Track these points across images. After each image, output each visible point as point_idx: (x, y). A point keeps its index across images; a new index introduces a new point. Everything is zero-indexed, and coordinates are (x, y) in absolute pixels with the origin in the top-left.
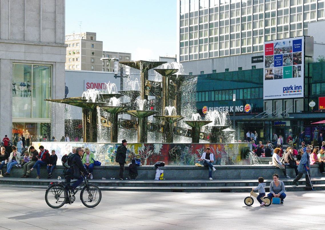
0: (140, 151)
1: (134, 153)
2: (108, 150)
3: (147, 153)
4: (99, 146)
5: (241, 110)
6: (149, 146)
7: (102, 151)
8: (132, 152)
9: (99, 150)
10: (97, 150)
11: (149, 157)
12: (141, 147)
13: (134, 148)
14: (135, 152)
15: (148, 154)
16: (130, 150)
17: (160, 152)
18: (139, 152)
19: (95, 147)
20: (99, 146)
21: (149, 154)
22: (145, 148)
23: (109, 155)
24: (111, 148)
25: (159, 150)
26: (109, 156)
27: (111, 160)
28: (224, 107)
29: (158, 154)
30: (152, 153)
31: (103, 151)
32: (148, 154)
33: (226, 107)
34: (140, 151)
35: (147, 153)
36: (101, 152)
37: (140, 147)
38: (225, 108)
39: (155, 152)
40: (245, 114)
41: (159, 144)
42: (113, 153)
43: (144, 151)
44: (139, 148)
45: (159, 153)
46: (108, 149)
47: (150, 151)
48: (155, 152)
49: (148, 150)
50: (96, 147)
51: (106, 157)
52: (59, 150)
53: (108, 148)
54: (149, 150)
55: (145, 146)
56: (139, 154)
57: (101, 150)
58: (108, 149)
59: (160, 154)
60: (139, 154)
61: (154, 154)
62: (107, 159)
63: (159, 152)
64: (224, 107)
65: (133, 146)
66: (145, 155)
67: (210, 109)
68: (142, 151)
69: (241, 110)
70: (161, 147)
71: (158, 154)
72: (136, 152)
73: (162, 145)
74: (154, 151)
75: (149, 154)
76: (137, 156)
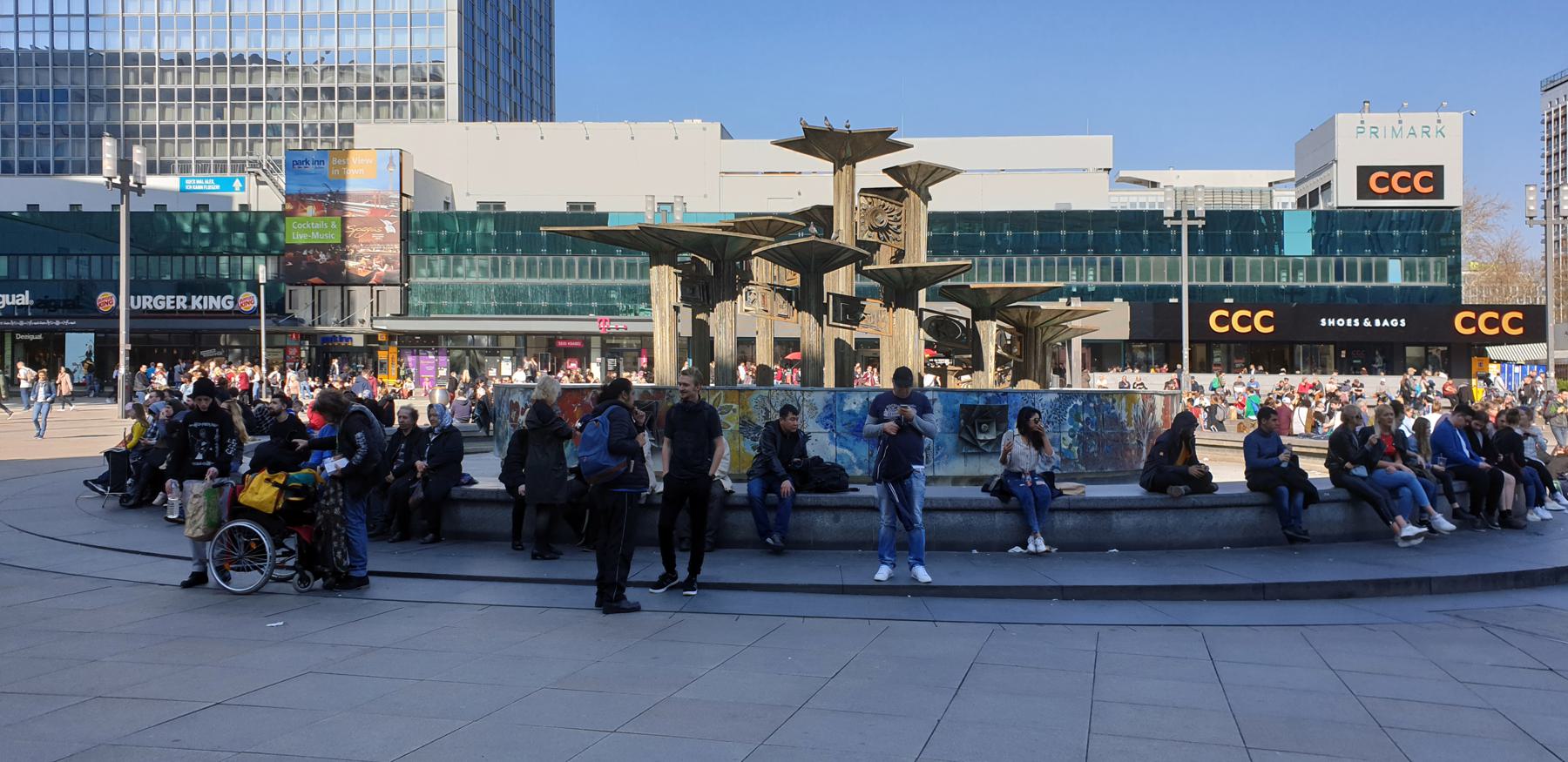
5: (228, 305)
7: (1051, 419)
13: (1125, 406)
24: (1075, 406)
28: (173, 297)
33: (179, 298)
36: (1048, 423)
38: (175, 299)
40: (237, 315)
42: (1080, 424)
46: (1068, 410)
51: (1064, 439)
57: (1050, 417)
58: (1068, 410)
64: (173, 297)
67: (148, 300)
69: (228, 305)
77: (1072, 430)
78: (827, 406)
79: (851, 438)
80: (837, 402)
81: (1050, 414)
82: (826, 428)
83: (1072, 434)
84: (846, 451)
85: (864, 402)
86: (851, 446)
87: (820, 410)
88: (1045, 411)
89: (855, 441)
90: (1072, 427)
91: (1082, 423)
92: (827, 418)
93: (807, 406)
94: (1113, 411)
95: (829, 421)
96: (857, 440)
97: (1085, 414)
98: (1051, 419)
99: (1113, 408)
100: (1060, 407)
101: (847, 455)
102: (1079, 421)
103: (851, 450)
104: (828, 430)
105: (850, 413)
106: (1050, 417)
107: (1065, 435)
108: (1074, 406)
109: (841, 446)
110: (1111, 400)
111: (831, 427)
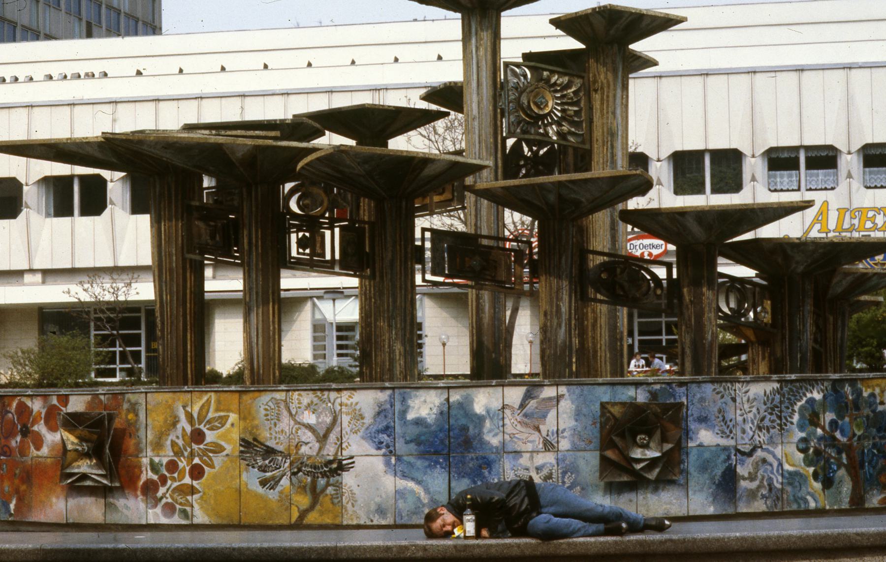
2: (796, 418)
4: (751, 394)
7: (767, 423)
9: (751, 415)
10: (740, 419)
19: (727, 399)
20: (751, 394)
23: (801, 446)
24: (811, 401)
26: (801, 451)
27: (811, 470)
31: (773, 421)
36: (760, 428)
42: (819, 431)
46: (796, 408)
50: (734, 400)
52: (465, 429)
53: (799, 404)
57: (762, 419)
62: (791, 469)
77: (804, 440)
78: (379, 413)
79: (419, 463)
80: (398, 407)
81: (762, 414)
82: (379, 448)
83: (803, 446)
84: (411, 485)
85: (442, 404)
86: (418, 475)
87: (368, 420)
88: (754, 410)
89: (426, 467)
90: (803, 435)
91: (823, 428)
92: (379, 432)
93: (348, 414)
95: (384, 437)
96: (429, 466)
98: (767, 423)
100: (781, 402)
101: (412, 492)
103: (419, 482)
104: (383, 450)
105: (419, 422)
106: (762, 419)
107: (792, 449)
108: (807, 402)
109: (404, 476)
110: (877, 391)
111: (388, 446)
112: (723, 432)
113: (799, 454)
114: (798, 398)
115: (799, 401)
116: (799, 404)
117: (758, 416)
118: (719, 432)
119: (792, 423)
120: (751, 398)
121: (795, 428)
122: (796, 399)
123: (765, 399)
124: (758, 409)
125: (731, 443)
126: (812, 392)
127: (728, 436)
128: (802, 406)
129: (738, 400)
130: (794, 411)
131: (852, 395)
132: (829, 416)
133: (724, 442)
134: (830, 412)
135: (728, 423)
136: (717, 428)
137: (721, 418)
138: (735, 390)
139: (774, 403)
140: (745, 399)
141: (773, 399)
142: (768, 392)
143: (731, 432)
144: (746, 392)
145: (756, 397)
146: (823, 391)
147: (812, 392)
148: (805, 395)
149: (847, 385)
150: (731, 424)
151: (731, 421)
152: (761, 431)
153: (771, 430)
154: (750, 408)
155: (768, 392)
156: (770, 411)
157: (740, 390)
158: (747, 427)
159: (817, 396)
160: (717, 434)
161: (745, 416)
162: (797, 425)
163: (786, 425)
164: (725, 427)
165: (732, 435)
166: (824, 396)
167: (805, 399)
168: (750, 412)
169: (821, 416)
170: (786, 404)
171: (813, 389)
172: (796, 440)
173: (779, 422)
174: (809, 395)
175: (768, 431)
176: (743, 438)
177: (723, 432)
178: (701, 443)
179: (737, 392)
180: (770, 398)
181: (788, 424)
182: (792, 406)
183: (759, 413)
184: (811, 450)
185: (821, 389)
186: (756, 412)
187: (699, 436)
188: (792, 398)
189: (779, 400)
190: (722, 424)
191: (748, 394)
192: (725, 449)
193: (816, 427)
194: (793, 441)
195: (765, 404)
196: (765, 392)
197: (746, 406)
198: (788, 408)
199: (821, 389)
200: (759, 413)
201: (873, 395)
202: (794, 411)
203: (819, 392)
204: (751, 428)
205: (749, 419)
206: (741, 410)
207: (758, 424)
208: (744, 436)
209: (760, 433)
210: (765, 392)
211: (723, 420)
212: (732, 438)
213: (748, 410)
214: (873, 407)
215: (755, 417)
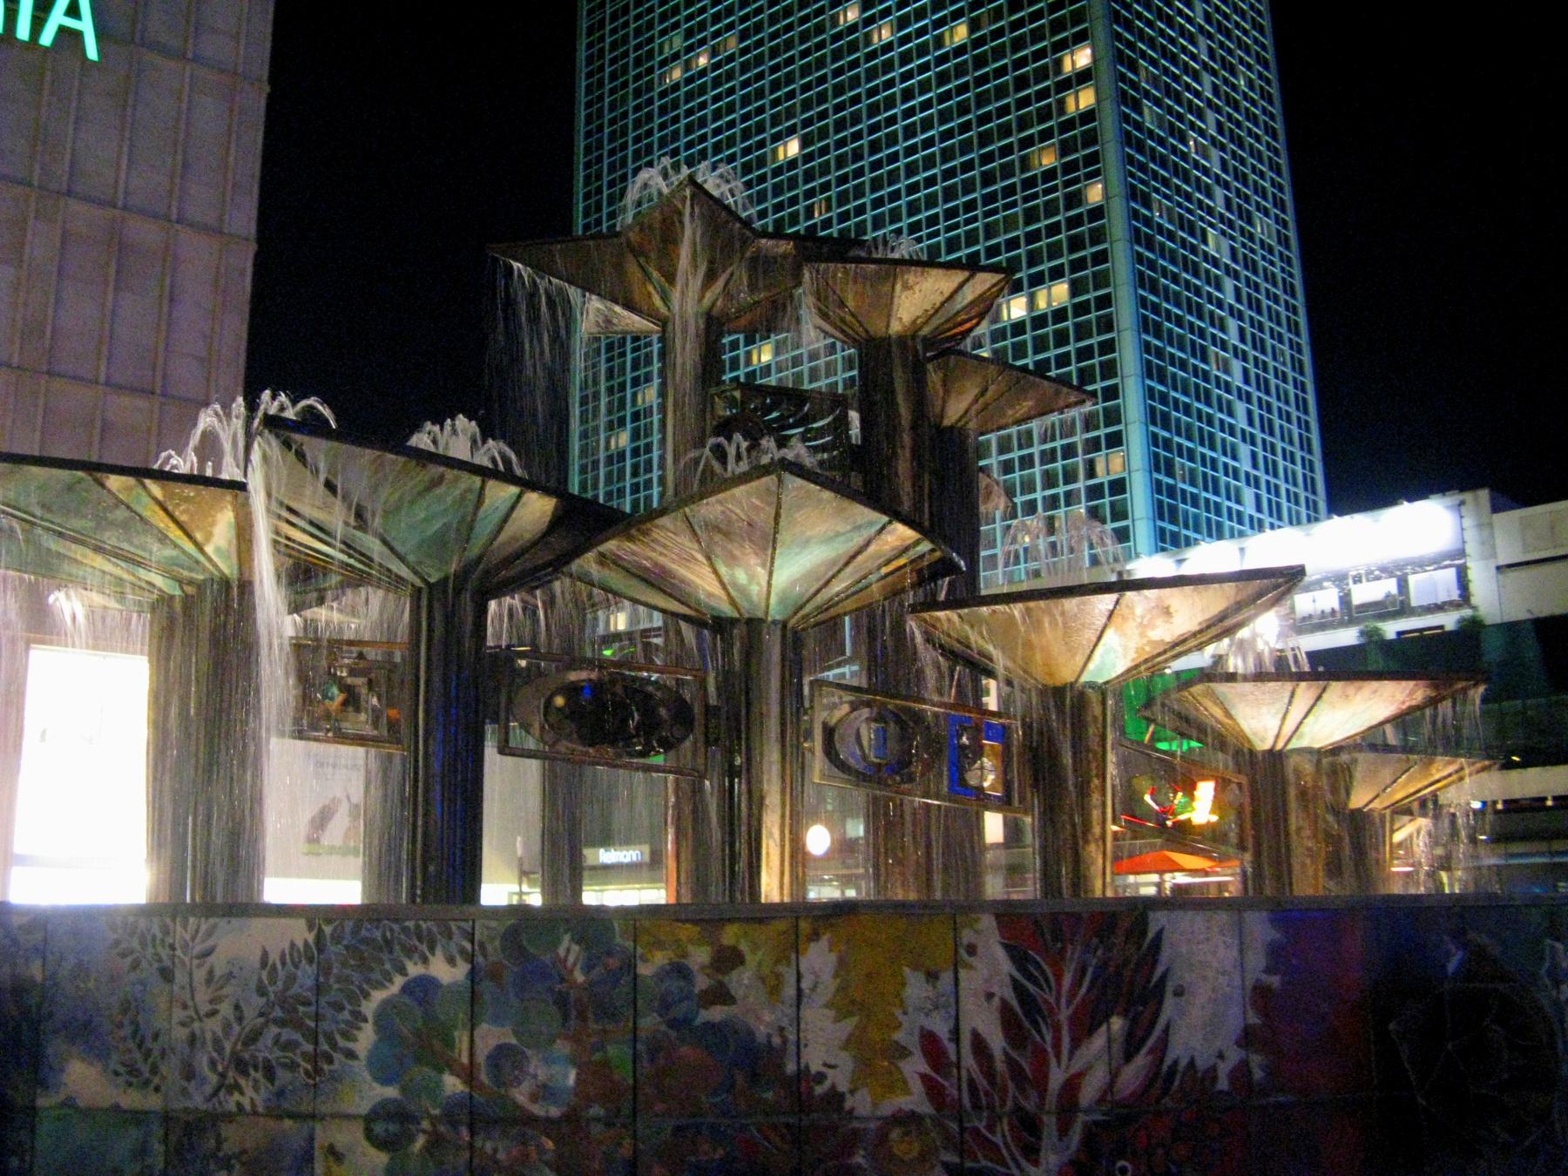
0: (930, 1044)
1: (840, 1079)
2: (366, 1038)
3: (1057, 1077)
4: (219, 962)
6: (1074, 954)
8: (802, 1074)
9: (213, 1026)
11: (1090, 1138)
12: (956, 965)
13: (829, 985)
14: (845, 1061)
15: (1072, 1086)
16: (761, 1031)
17: (1247, 1038)
18: (915, 1066)
21: (1088, 1093)
22: (1017, 986)
23: (379, 1128)
24: (423, 989)
25: (1236, 1018)
29: (1223, 1084)
30: (1133, 1074)
31: (290, 1046)
32: (1072, 1086)
34: (930, 1044)
35: (1057, 1077)
36: (242, 1066)
37: (932, 976)
39: (1178, 1050)
41: (1223, 917)
42: (452, 1084)
43: (997, 1042)
44: (916, 989)
45: (1242, 1069)
46: (369, 1007)
47: (1098, 1041)
48: (1178, 1050)
49: (1064, 1015)
51: (333, 1153)
53: (378, 996)
54: (1086, 1025)
55: (1018, 956)
56: (914, 1099)
57: (253, 1038)
58: (369, 1007)
59: (1258, 1074)
60: (914, 1099)
61: (1161, 1078)
63: (1234, 1056)
65: (819, 959)
66: (1030, 1105)
68: (979, 1045)
70: (1257, 960)
71: (1223, 1084)
72: (865, 1069)
73: (1272, 934)
74: (1163, 1044)
75: (1088, 1093)
76: (882, 1137)
77: (382, 1112)
88: (226, 1009)
90: (391, 1092)
91: (469, 1075)
94: (716, 1014)
97: (484, 1028)
98: (265, 1049)
99: (720, 995)
100: (319, 989)
102: (451, 1066)
106: (253, 1038)
107: (349, 1137)
108: (405, 989)
110: (700, 956)
112: (133, 1071)
113: (372, 1151)
114: (376, 976)
115: (380, 985)
116: (378, 996)
117: (237, 1028)
118: (122, 1070)
119: (351, 1055)
120: (218, 973)
121: (360, 1068)
122: (368, 981)
123: (264, 975)
124: (237, 1007)
125: (153, 1102)
126: (425, 960)
127: (146, 1083)
128: (387, 1004)
129: (180, 977)
130: (359, 1017)
131: (588, 968)
132: (490, 1036)
133: (132, 1099)
134: (497, 1020)
135: (149, 1044)
136: (115, 1057)
137: (127, 1030)
138: (172, 947)
139: (295, 990)
140: (200, 975)
141: (291, 979)
142: (274, 957)
143: (154, 1070)
144: (208, 953)
145: (236, 971)
146: (470, 958)
147: (425, 960)
148: (402, 971)
149: (567, 938)
150: (156, 1048)
151: (156, 1036)
152: (245, 1073)
153: (283, 1076)
154: (211, 1002)
155: (274, 957)
156: (278, 1013)
157: (185, 946)
158: (202, 1062)
159: (446, 971)
160: (116, 1073)
161: (196, 1025)
162: (370, 1063)
163: (330, 1061)
164: (138, 1056)
165: (156, 1080)
166: (473, 974)
167: (399, 981)
168: (213, 1013)
169: (462, 1039)
170: (334, 994)
171: (432, 949)
172: (364, 1108)
173: (309, 1048)
174: (414, 969)
175: (269, 1072)
176: (184, 1092)
177: (133, 1071)
178: (69, 1098)
179: (179, 952)
180: (281, 973)
181: (337, 1056)
182: (353, 999)
183: (240, 1019)
184: (420, 1142)
185: (462, 951)
186: (232, 1018)
187: (65, 1078)
188: (356, 977)
189: (310, 982)
190: (131, 1045)
191: (212, 959)
192: (138, 1117)
193: (441, 1071)
194: (352, 1110)
195: (262, 991)
196: (265, 954)
197: (202, 997)
198: (340, 1008)
199: (462, 951)
200: (240, 1019)
201: (679, 971)
202: (359, 1017)
203: (451, 961)
204: (213, 1063)
205: (209, 1036)
206: (185, 1007)
207: (234, 1053)
208: (191, 1086)
209: (242, 1082)
210: (265, 954)
211: (135, 1034)
212: (157, 1089)
213: (205, 1008)
214: (679, 1011)
215: (227, 1027)
